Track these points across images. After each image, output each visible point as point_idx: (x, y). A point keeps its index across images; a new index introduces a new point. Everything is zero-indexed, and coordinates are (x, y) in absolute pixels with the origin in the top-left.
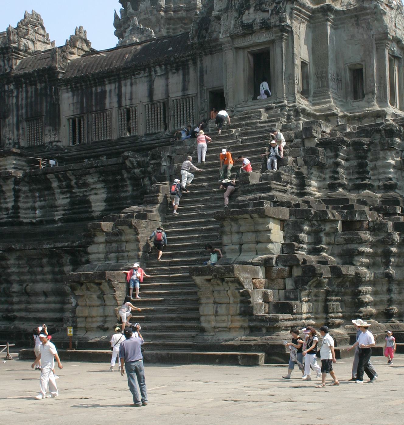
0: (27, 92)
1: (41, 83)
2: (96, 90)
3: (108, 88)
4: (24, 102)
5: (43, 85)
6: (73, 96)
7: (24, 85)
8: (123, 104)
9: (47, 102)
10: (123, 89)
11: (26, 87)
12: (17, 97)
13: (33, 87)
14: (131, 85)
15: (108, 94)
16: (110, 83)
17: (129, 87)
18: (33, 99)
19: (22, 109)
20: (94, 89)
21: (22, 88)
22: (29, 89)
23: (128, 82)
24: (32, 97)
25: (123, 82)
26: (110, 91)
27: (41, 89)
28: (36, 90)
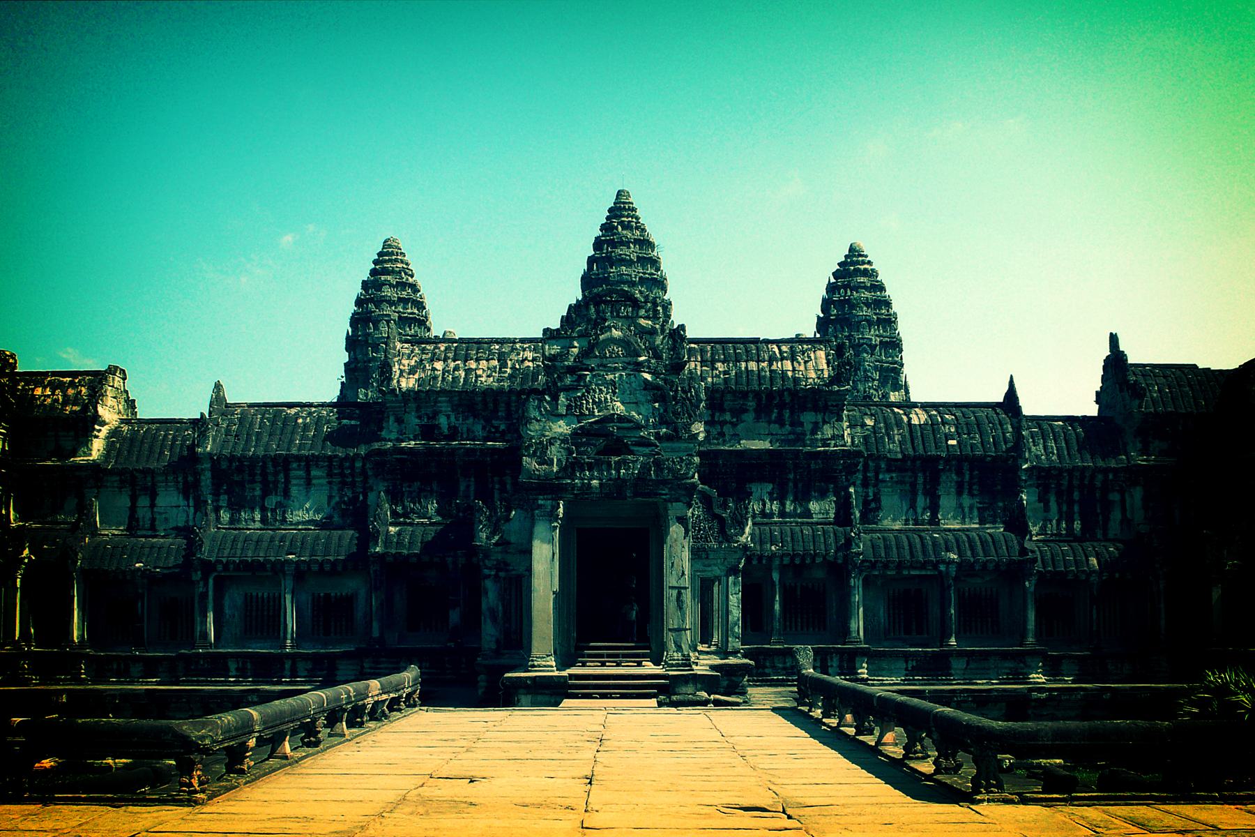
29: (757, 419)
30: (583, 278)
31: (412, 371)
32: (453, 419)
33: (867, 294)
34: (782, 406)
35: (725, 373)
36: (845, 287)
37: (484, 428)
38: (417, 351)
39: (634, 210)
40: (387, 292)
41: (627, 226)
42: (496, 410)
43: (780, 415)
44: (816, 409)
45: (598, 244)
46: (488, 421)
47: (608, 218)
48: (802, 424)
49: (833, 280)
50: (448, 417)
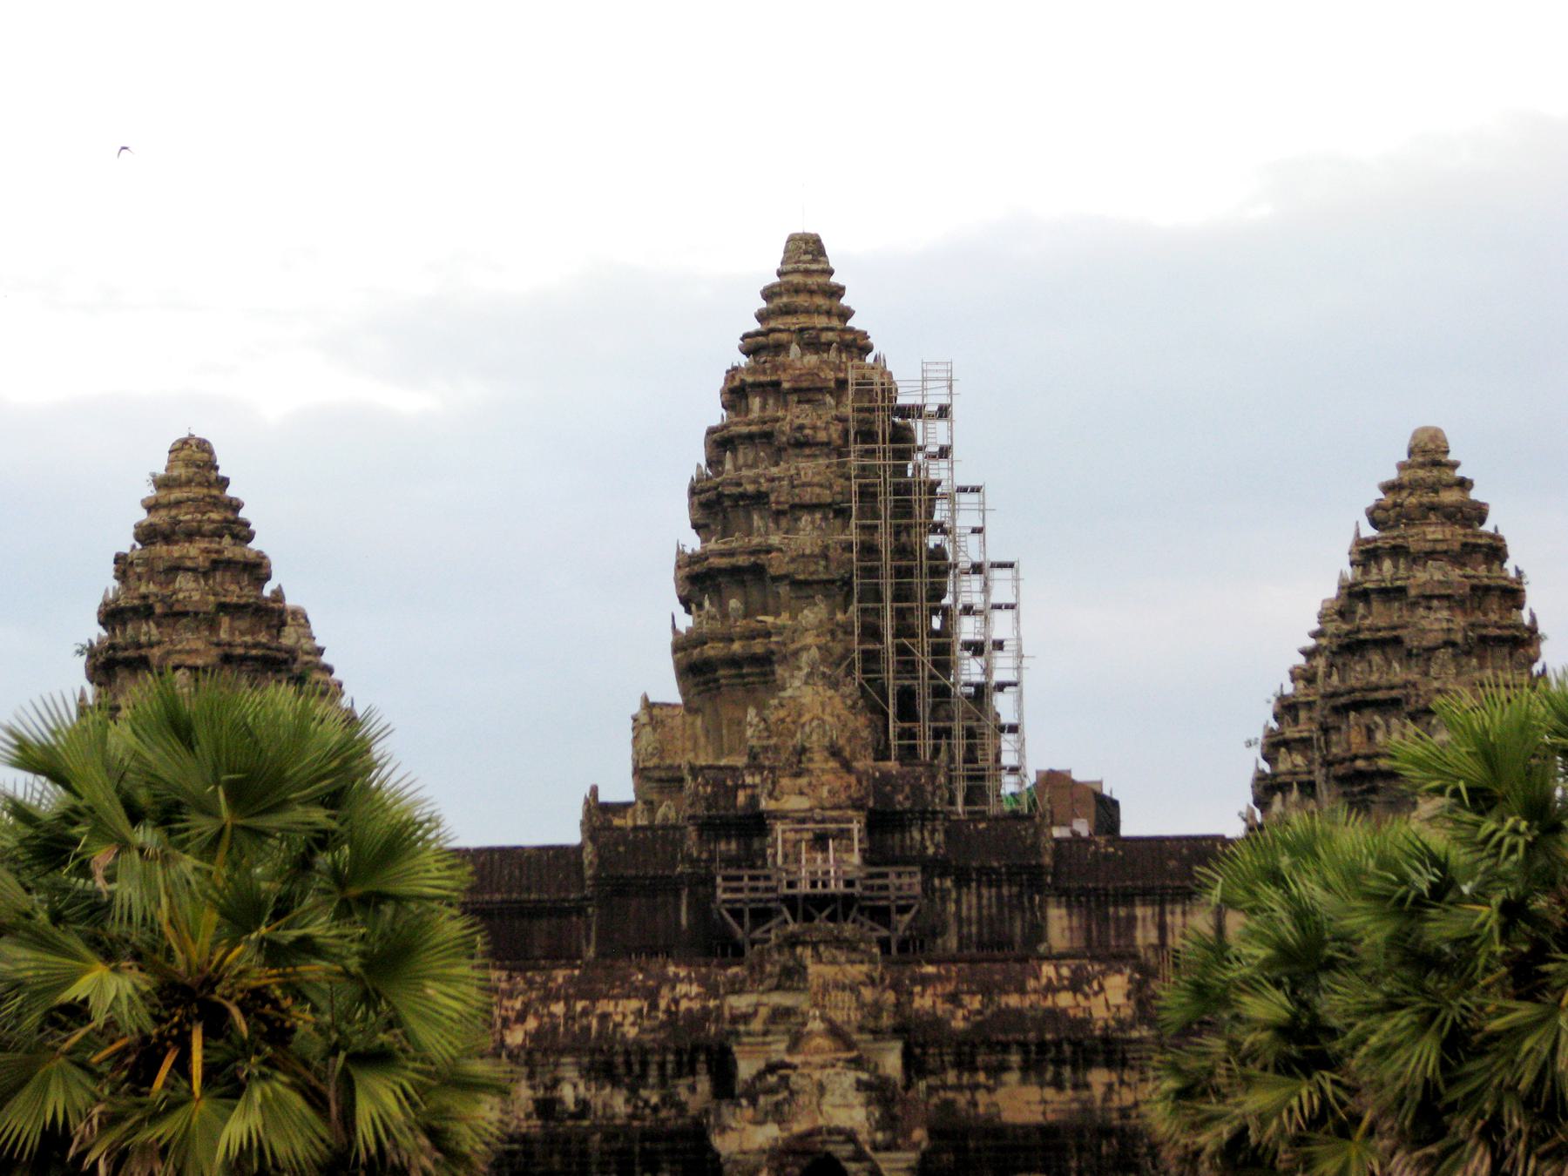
0: (980, 897)
1: (1010, 886)
2: (1116, 913)
3: (1139, 912)
4: (974, 913)
5: (1015, 890)
6: (1070, 915)
7: (974, 885)
8: (1170, 941)
9: (1023, 920)
10: (1169, 918)
11: (979, 887)
12: (958, 902)
13: (994, 891)
14: (1184, 913)
15: (1139, 924)
16: (1144, 905)
17: (1179, 919)
18: (994, 910)
19: (970, 924)
20: (1111, 910)
21: (969, 888)
22: (985, 891)
23: (1178, 909)
24: (990, 906)
25: (1168, 908)
26: (1144, 919)
27: (1010, 896)
28: (999, 896)
29: (1024, 1081)
30: (693, 492)
31: (521, 1018)
32: (581, 1088)
33: (1455, 574)
34: (1059, 1062)
35: (979, 1012)
36: (1397, 552)
37: (627, 1101)
38: (521, 985)
39: (838, 292)
40: (188, 589)
41: (813, 344)
42: (643, 1075)
43: (1058, 1075)
44: (1109, 1064)
45: (736, 394)
46: (633, 1090)
47: (762, 317)
48: (1087, 1086)
49: (1369, 531)
50: (575, 1086)
